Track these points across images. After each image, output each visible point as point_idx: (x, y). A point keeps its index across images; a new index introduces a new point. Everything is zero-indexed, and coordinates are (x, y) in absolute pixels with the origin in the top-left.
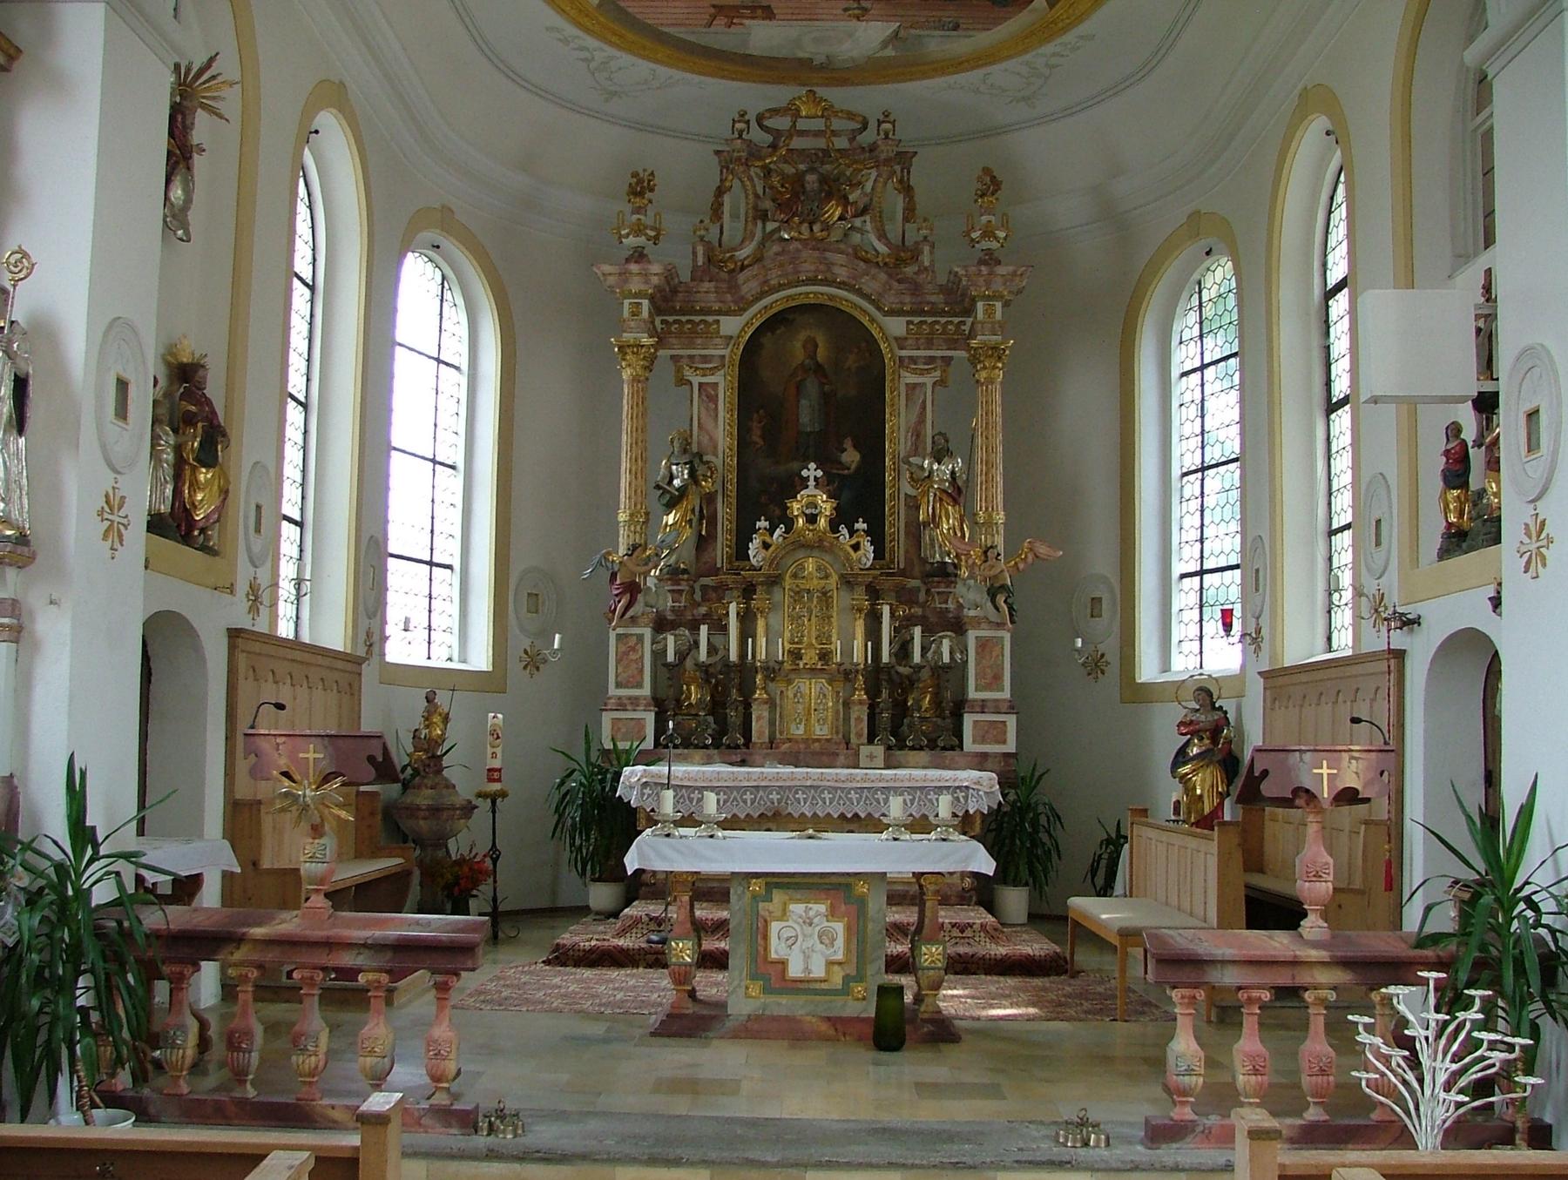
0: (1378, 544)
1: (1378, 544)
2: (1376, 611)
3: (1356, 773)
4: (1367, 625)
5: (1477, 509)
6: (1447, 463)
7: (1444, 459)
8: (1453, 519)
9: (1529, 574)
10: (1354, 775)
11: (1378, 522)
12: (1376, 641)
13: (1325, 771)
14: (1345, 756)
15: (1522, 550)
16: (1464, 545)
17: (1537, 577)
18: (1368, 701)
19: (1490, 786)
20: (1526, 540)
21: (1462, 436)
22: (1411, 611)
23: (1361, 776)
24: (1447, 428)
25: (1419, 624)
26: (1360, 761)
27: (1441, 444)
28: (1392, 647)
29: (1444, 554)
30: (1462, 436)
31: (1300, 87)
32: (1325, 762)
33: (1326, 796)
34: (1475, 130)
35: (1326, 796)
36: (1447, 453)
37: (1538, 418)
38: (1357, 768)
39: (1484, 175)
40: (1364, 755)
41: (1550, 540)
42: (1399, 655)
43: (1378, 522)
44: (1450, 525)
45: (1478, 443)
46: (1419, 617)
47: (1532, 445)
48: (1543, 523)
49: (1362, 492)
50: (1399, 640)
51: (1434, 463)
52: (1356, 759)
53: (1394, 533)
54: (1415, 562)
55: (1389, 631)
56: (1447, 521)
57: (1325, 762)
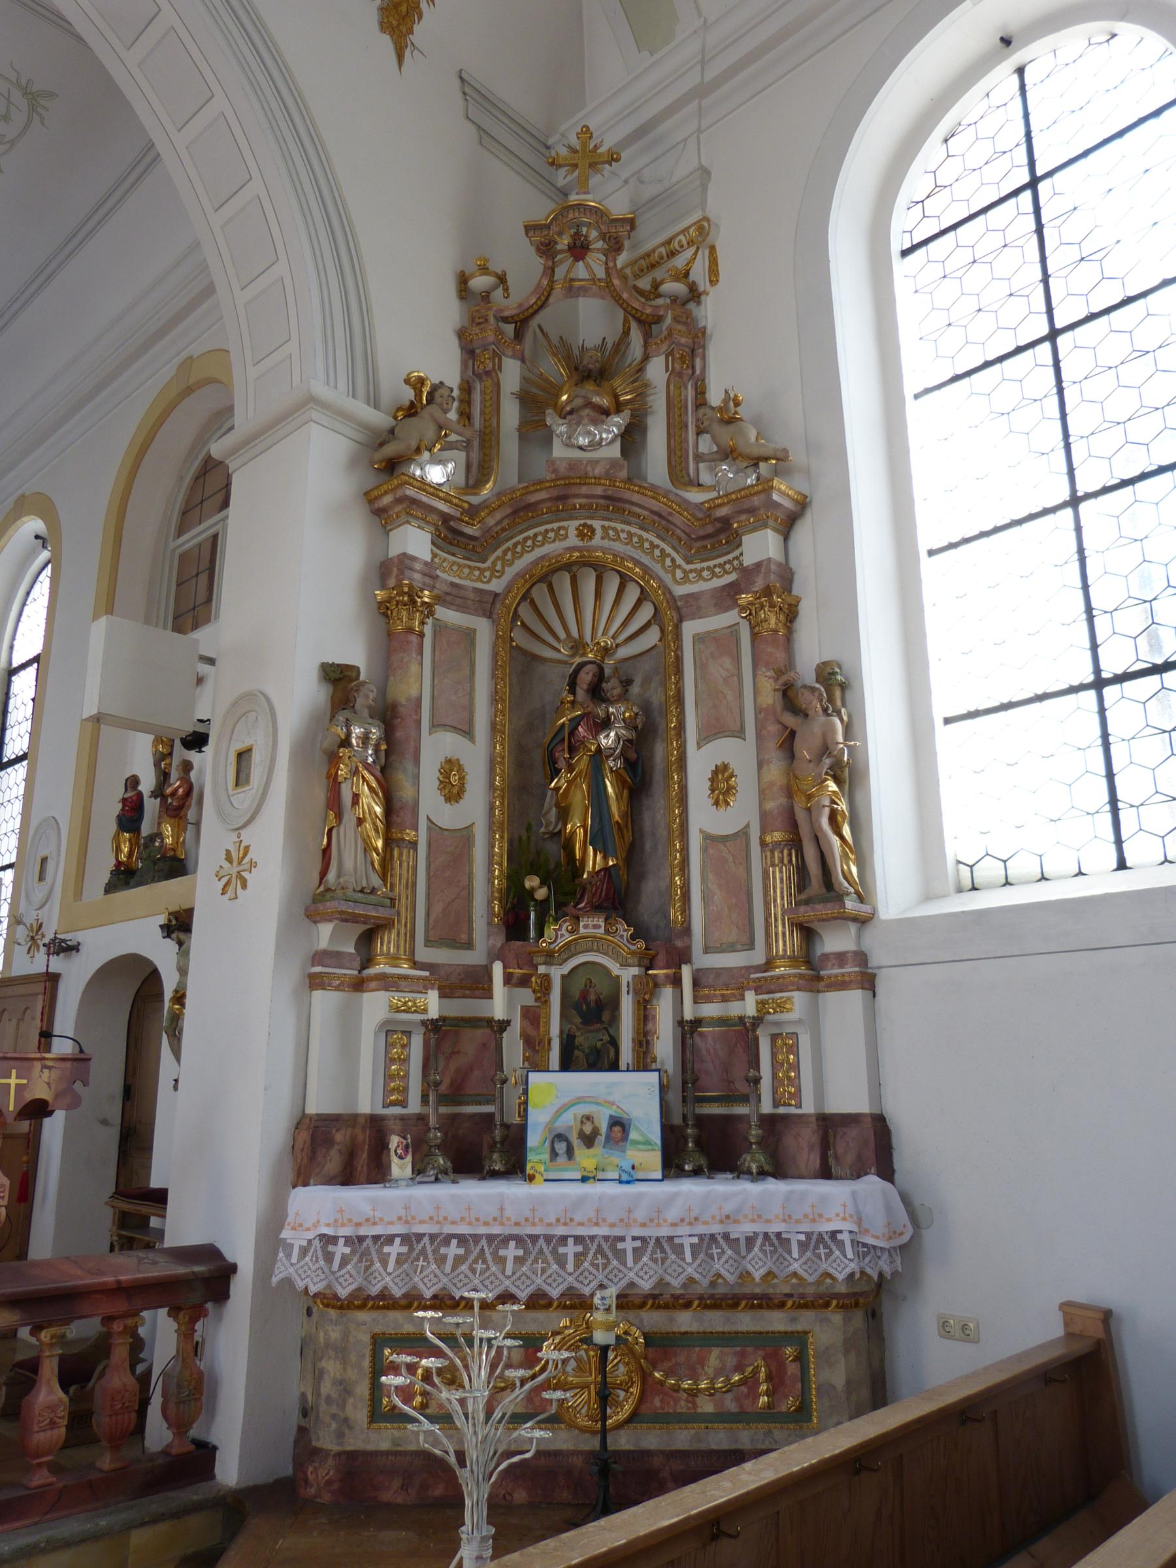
0: (41, 878)
1: (41, 878)
2: (32, 938)
3: (48, 1084)
4: (20, 952)
5: (148, 850)
6: (122, 810)
7: (120, 805)
8: (123, 858)
9: (227, 896)
10: (46, 1086)
11: (44, 860)
12: (38, 963)
13: (13, 1081)
14: (38, 1065)
15: (221, 874)
16: (132, 882)
17: (236, 898)
18: (14, 1021)
19: (128, 1099)
20: (226, 865)
21: (140, 788)
22: (71, 937)
23: (53, 1086)
24: (127, 780)
25: (78, 950)
26: (53, 1071)
27: (119, 792)
28: (50, 970)
29: (110, 888)
30: (140, 788)
31: (20, 492)
32: (14, 1072)
33: (11, 1108)
34: (174, 550)
35: (11, 1108)
36: (124, 801)
37: (251, 757)
38: (49, 1078)
39: (178, 585)
40: (57, 1064)
41: (253, 865)
42: (52, 979)
43: (44, 860)
44: (119, 864)
45: (154, 794)
46: (79, 944)
47: (241, 778)
48: (247, 848)
49: (30, 839)
50: (57, 964)
51: (109, 808)
52: (49, 1068)
53: (58, 872)
54: (79, 894)
55: (48, 956)
56: (117, 859)
57: (14, 1072)
